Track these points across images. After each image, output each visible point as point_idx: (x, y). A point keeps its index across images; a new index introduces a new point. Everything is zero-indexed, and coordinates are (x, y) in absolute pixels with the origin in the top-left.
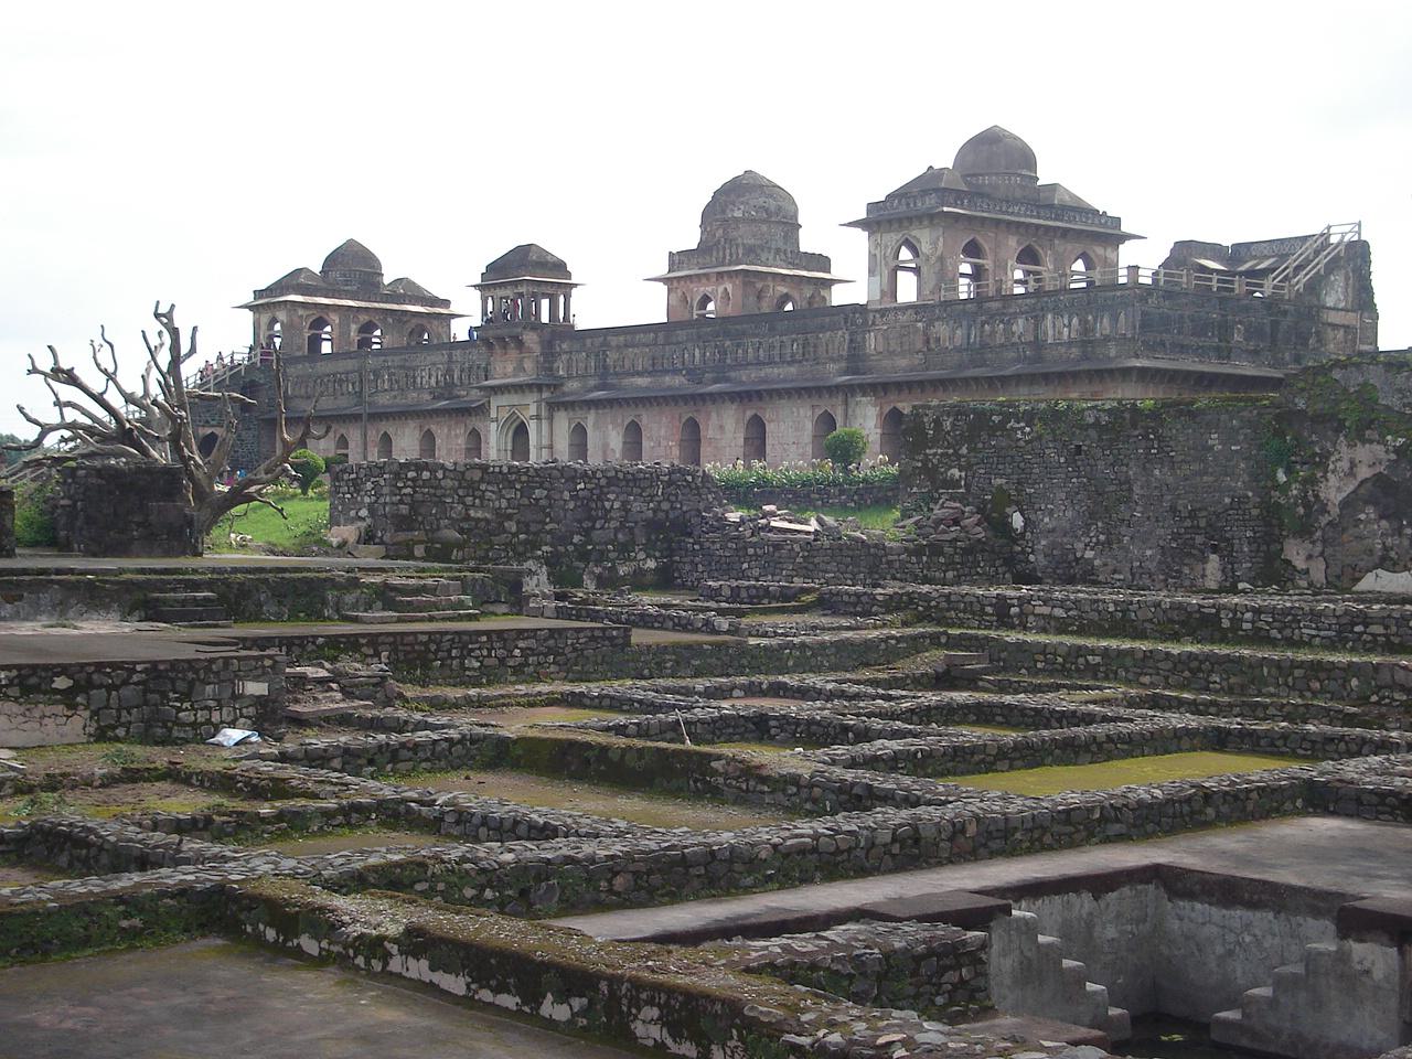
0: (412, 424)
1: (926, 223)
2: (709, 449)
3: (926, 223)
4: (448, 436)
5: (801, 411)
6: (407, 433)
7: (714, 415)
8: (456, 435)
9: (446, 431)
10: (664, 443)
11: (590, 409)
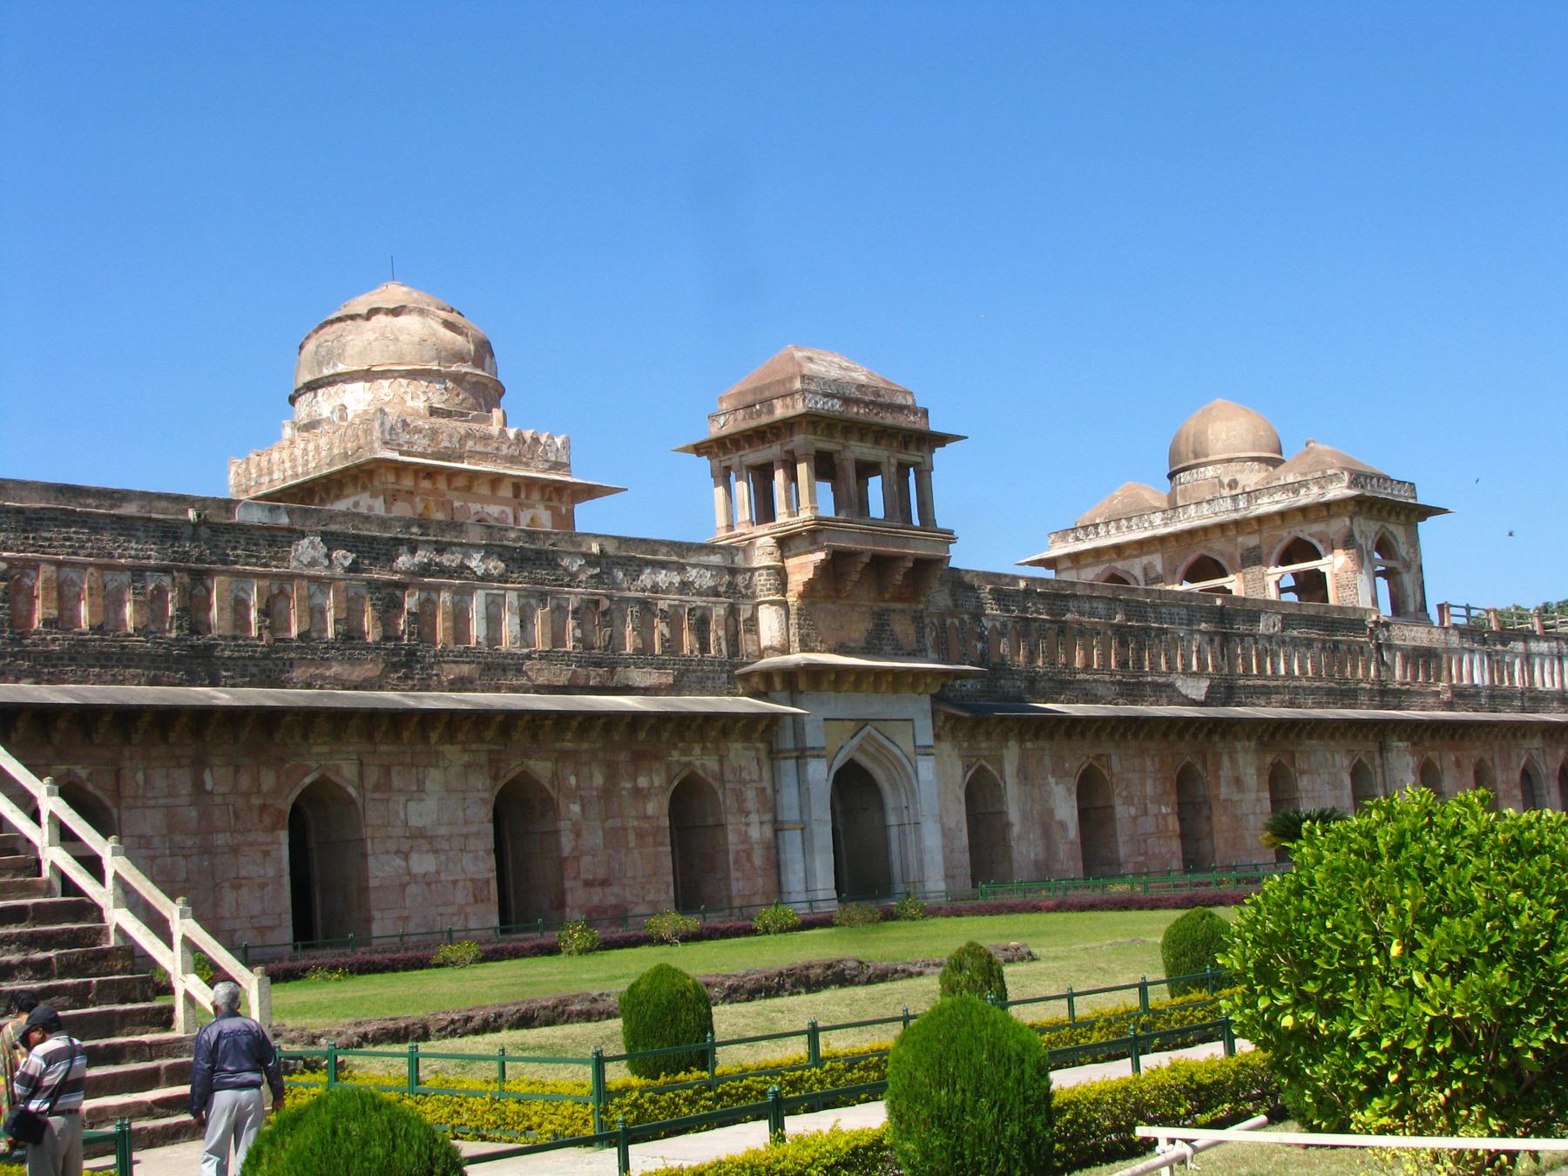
0: (453, 753)
1: (1402, 517)
2: (1224, 819)
3: (1402, 517)
4: (607, 793)
5: (1337, 757)
6: (429, 785)
7: (1226, 761)
8: (636, 791)
9: (599, 780)
10: (1152, 809)
11: (1006, 739)
